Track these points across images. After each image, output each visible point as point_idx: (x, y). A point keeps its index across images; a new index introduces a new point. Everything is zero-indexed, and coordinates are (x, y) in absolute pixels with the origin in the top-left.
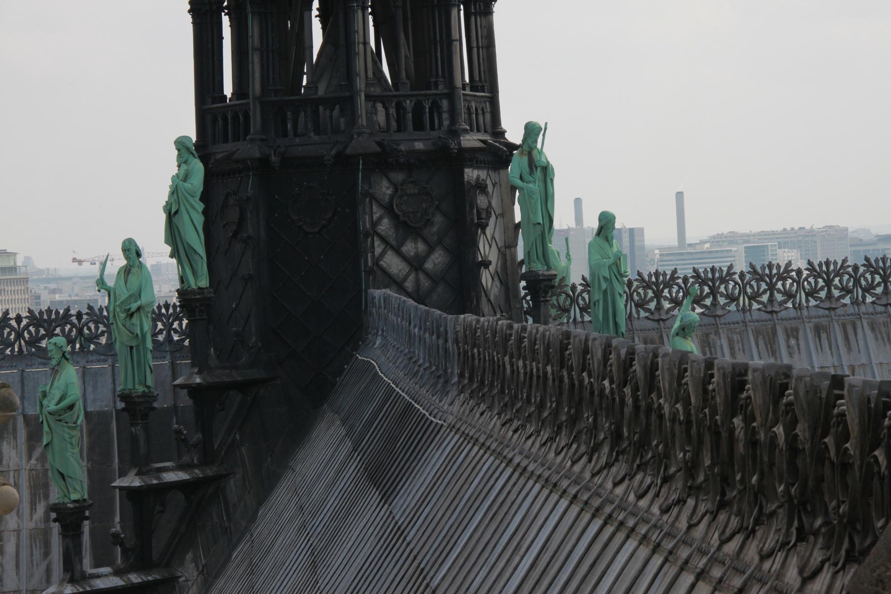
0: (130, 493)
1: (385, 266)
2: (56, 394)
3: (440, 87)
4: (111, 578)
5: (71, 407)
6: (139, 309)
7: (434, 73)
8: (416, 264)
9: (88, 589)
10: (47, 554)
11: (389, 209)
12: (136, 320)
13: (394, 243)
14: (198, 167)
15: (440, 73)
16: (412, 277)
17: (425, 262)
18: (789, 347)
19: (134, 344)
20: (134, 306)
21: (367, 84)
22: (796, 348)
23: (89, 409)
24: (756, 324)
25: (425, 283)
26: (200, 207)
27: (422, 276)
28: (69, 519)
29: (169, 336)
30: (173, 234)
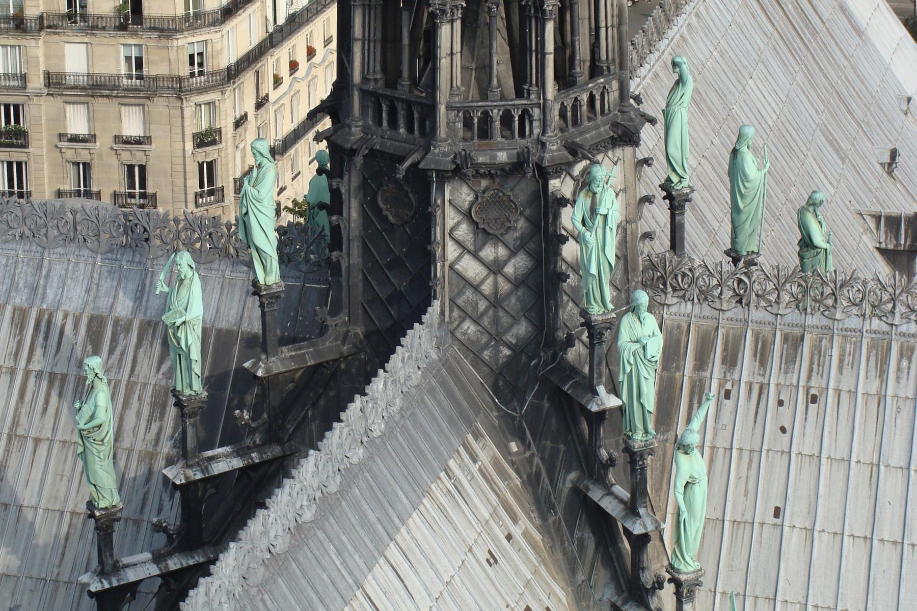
1: (461, 269)
3: (533, 96)
7: (529, 80)
8: (495, 268)
11: (467, 215)
13: (472, 248)
15: (534, 82)
16: (490, 280)
17: (504, 267)
18: (899, 369)
20: (179, 322)
21: (451, 94)
22: (906, 371)
24: (874, 336)
25: (504, 286)
27: (500, 280)
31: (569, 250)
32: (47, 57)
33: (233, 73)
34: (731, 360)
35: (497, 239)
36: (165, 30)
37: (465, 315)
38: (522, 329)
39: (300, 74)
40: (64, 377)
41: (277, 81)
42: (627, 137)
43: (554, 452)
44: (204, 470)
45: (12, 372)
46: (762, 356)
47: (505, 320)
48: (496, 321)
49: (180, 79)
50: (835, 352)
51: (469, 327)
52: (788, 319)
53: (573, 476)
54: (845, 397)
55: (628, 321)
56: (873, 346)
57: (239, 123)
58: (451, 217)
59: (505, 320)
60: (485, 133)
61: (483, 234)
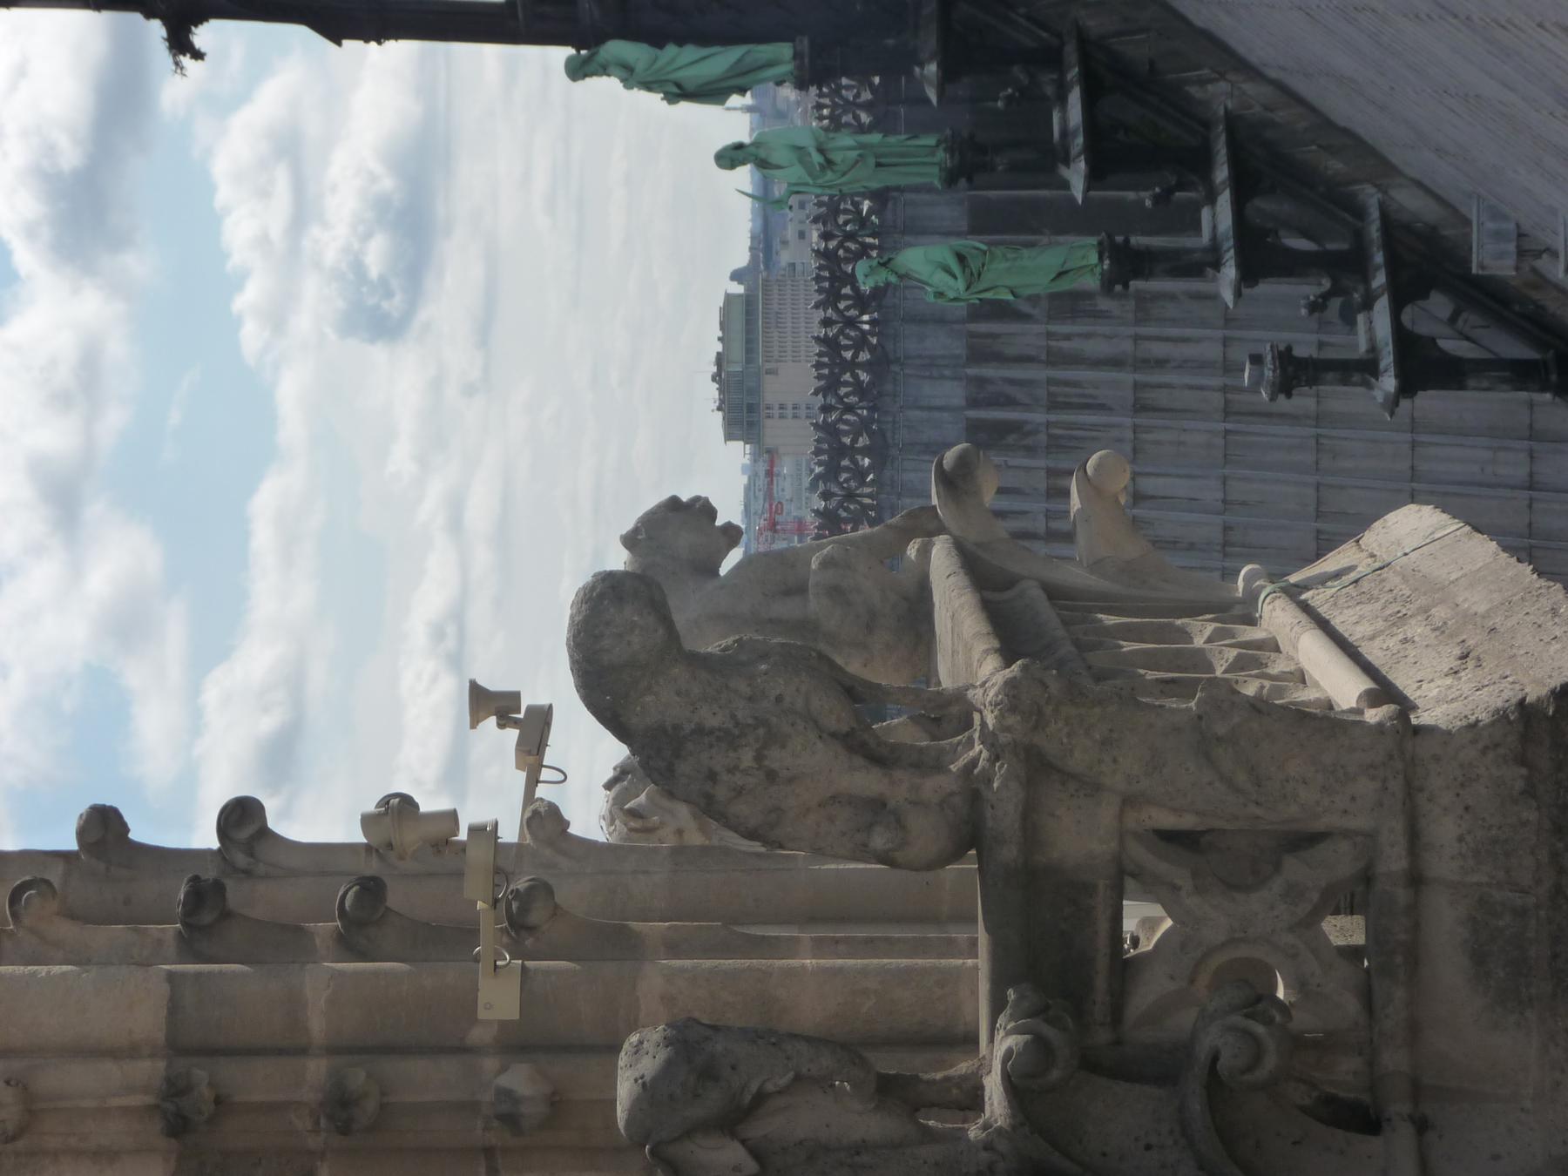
0: (1095, 177)
2: (940, 279)
4: (1218, 208)
5: (961, 258)
6: (821, 151)
9: (1231, 242)
10: (1172, 297)
12: (837, 157)
14: (616, 48)
19: (872, 161)
20: (817, 158)
23: (963, 403)
26: (671, 50)
28: (1127, 265)
29: (862, 366)
30: (711, 93)
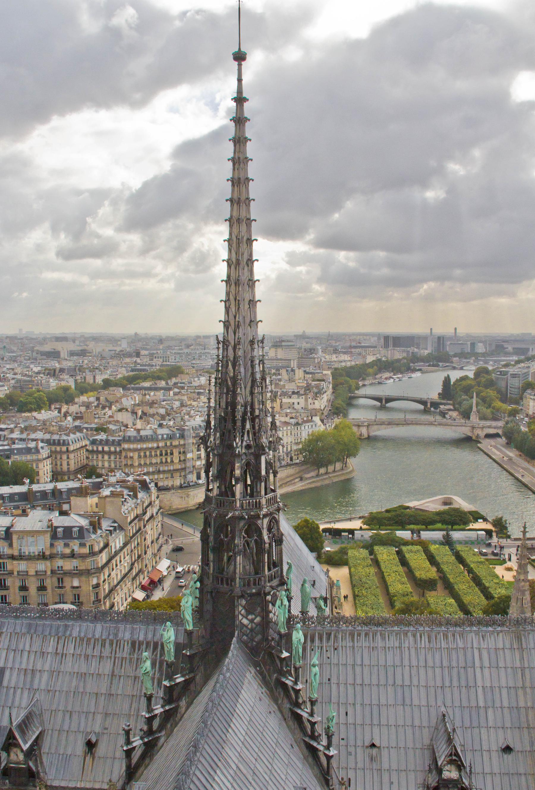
2: (144, 668)
8: (252, 621)
10: (153, 685)
11: (244, 607)
25: (254, 625)
31: (271, 615)
32: (51, 565)
33: (103, 567)
34: (312, 641)
35: (252, 613)
36: (83, 557)
37: (244, 634)
38: (259, 637)
39: (118, 567)
40: (126, 658)
41: (113, 569)
42: (283, 583)
43: (269, 669)
44: (175, 681)
45: (111, 657)
46: (321, 639)
47: (254, 635)
48: (252, 635)
49: (89, 570)
50: (340, 637)
51: (245, 638)
52: (327, 628)
53: (275, 675)
54: (344, 648)
55: (294, 633)
56: (349, 635)
57: (104, 581)
58: (240, 608)
59: (254, 635)
60: (249, 585)
61: (249, 612)
